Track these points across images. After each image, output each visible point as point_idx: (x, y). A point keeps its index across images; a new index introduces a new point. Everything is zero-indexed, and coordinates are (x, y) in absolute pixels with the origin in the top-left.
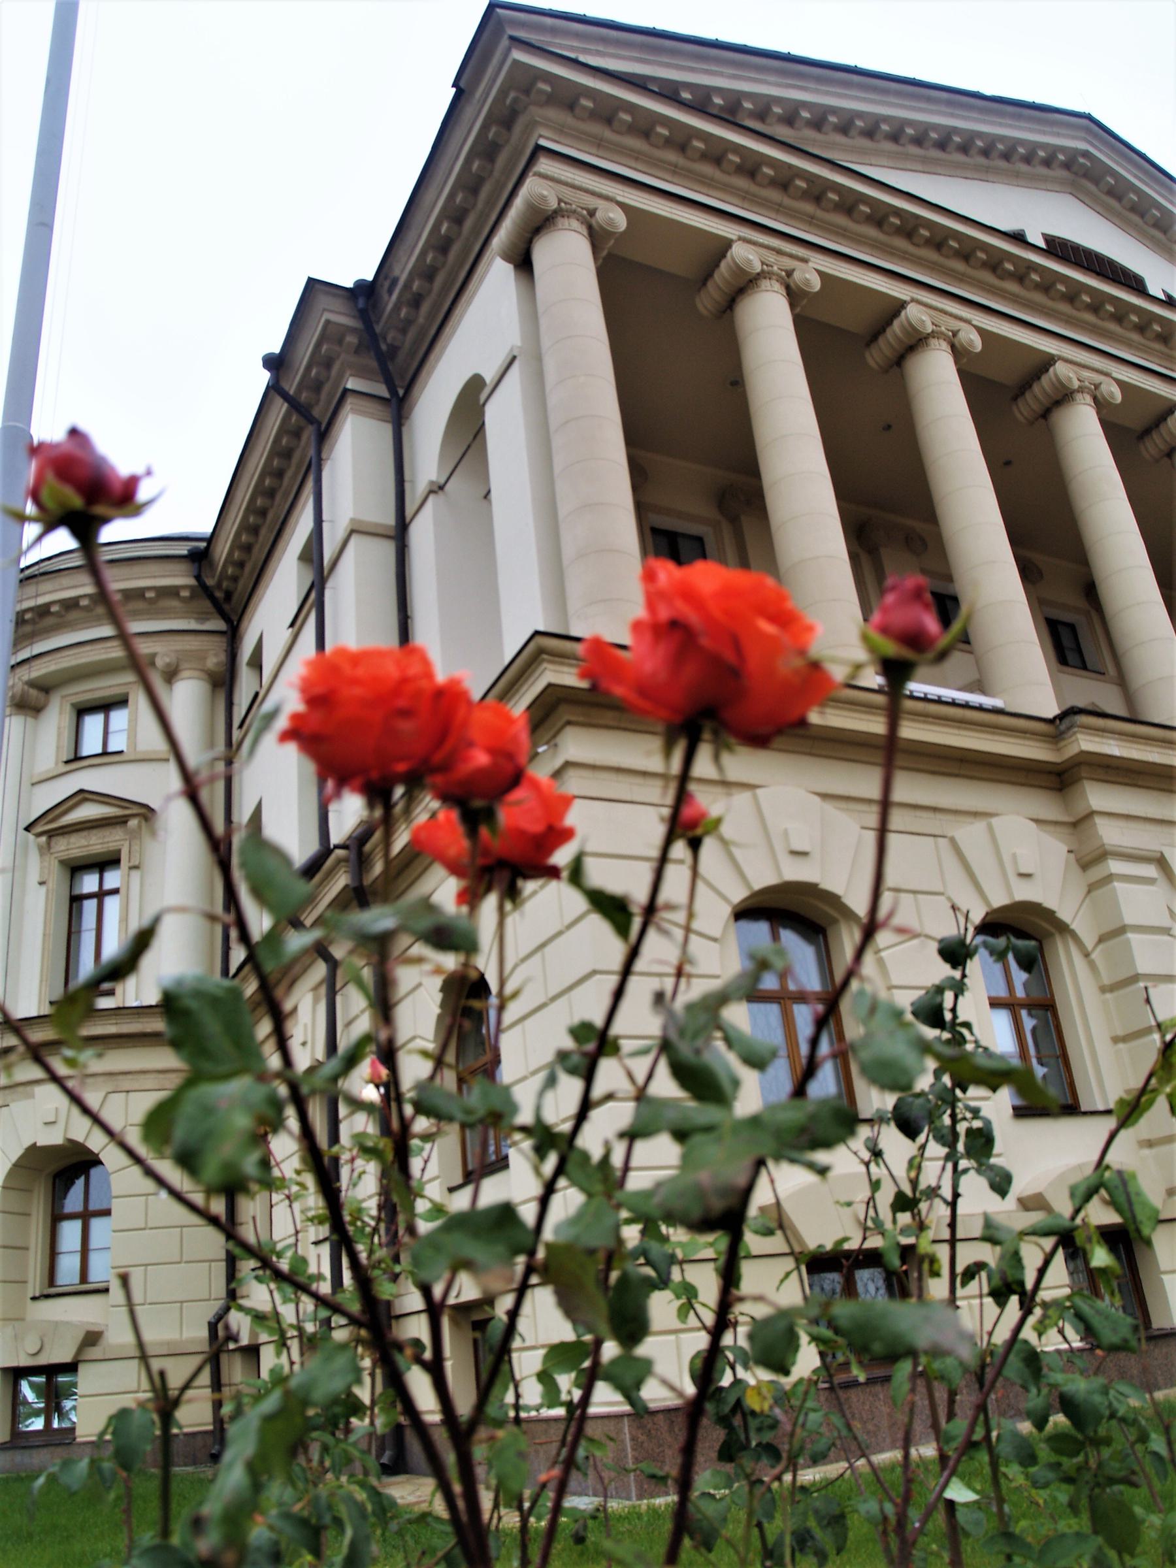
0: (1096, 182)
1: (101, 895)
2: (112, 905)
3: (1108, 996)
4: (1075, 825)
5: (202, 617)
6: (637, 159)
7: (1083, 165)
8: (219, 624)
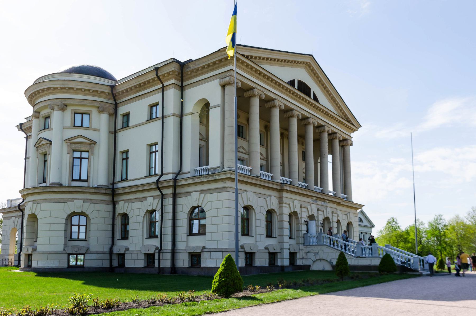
1: (81, 158)
2: (85, 162)
4: (280, 197)
5: (108, 99)
8: (112, 101)
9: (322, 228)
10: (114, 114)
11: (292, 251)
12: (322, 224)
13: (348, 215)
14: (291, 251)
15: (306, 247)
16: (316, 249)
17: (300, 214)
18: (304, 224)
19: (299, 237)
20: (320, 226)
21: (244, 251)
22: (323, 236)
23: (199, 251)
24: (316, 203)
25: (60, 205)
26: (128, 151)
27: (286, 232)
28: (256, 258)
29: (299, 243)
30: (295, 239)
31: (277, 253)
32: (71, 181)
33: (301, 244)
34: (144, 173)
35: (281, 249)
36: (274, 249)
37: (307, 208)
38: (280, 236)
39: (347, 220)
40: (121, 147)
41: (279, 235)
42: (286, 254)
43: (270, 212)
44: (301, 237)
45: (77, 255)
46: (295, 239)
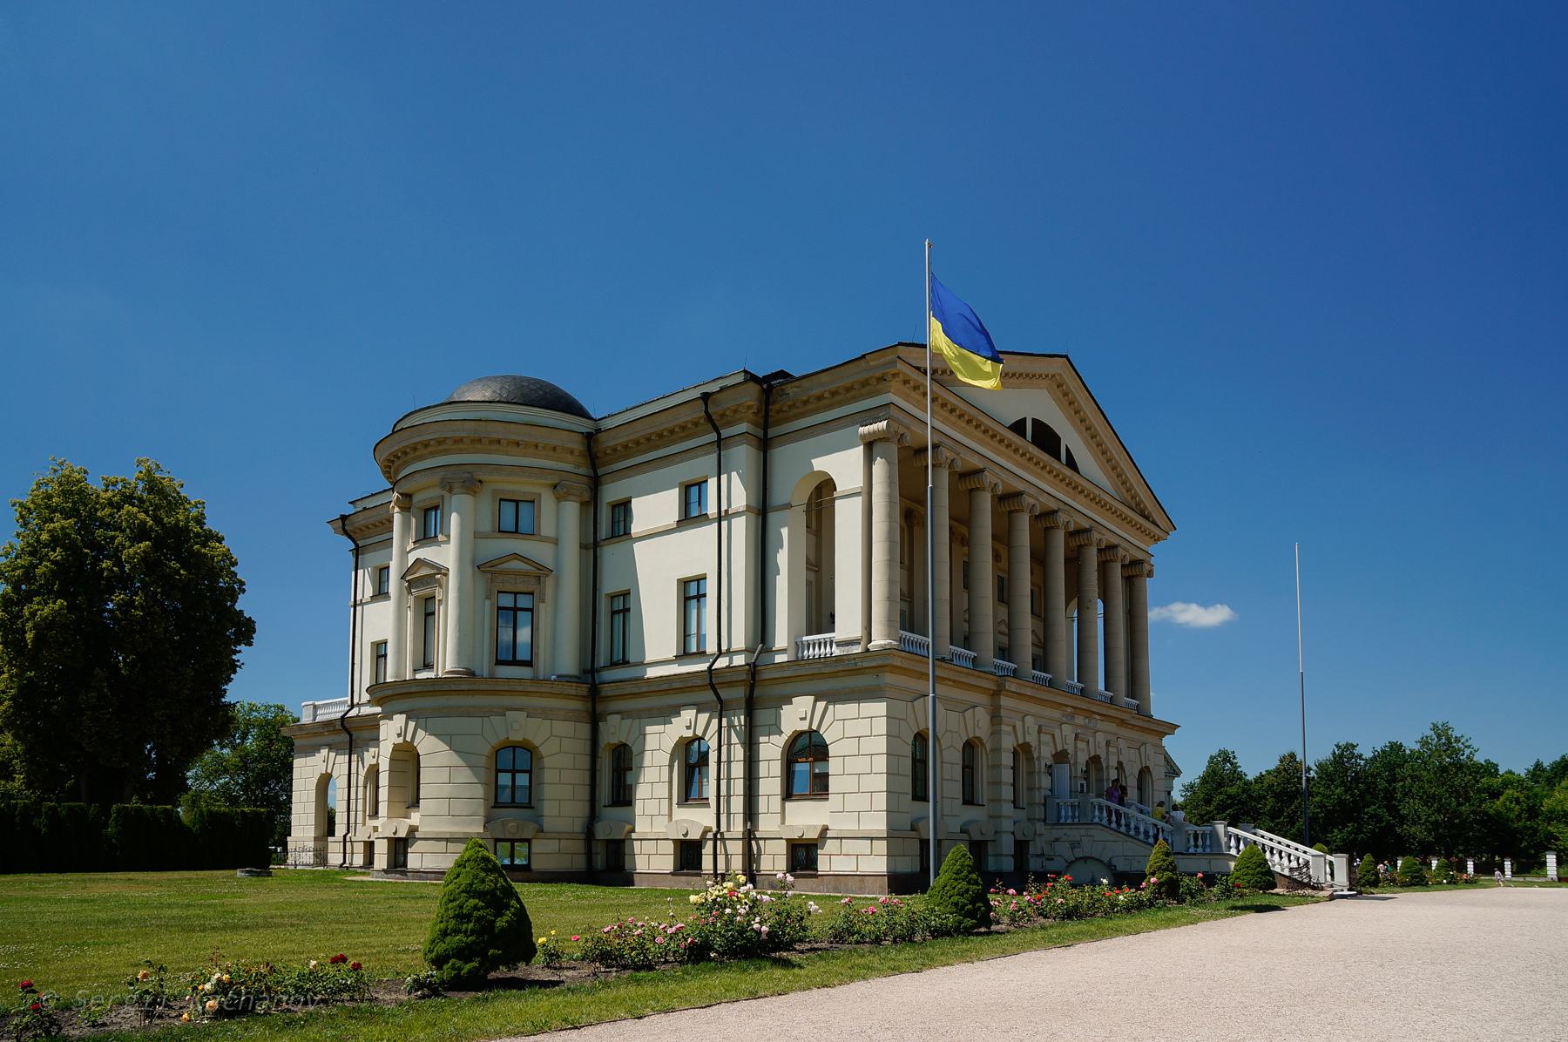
1: (515, 610)
9: (1085, 783)
10: (591, 503)
11: (1020, 837)
12: (1085, 772)
13: (1142, 749)
14: (1018, 838)
15: (1049, 827)
16: (1075, 834)
19: (1035, 804)
22: (1092, 803)
23: (814, 835)
24: (1072, 722)
25: (474, 724)
26: (629, 594)
27: (1007, 792)
29: (1034, 819)
32: (496, 664)
33: (1039, 820)
34: (671, 651)
35: (996, 832)
36: (982, 834)
37: (1053, 735)
38: (993, 801)
39: (1139, 762)
40: (610, 585)
42: (1007, 845)
43: (970, 747)
44: (1039, 804)
45: (513, 841)
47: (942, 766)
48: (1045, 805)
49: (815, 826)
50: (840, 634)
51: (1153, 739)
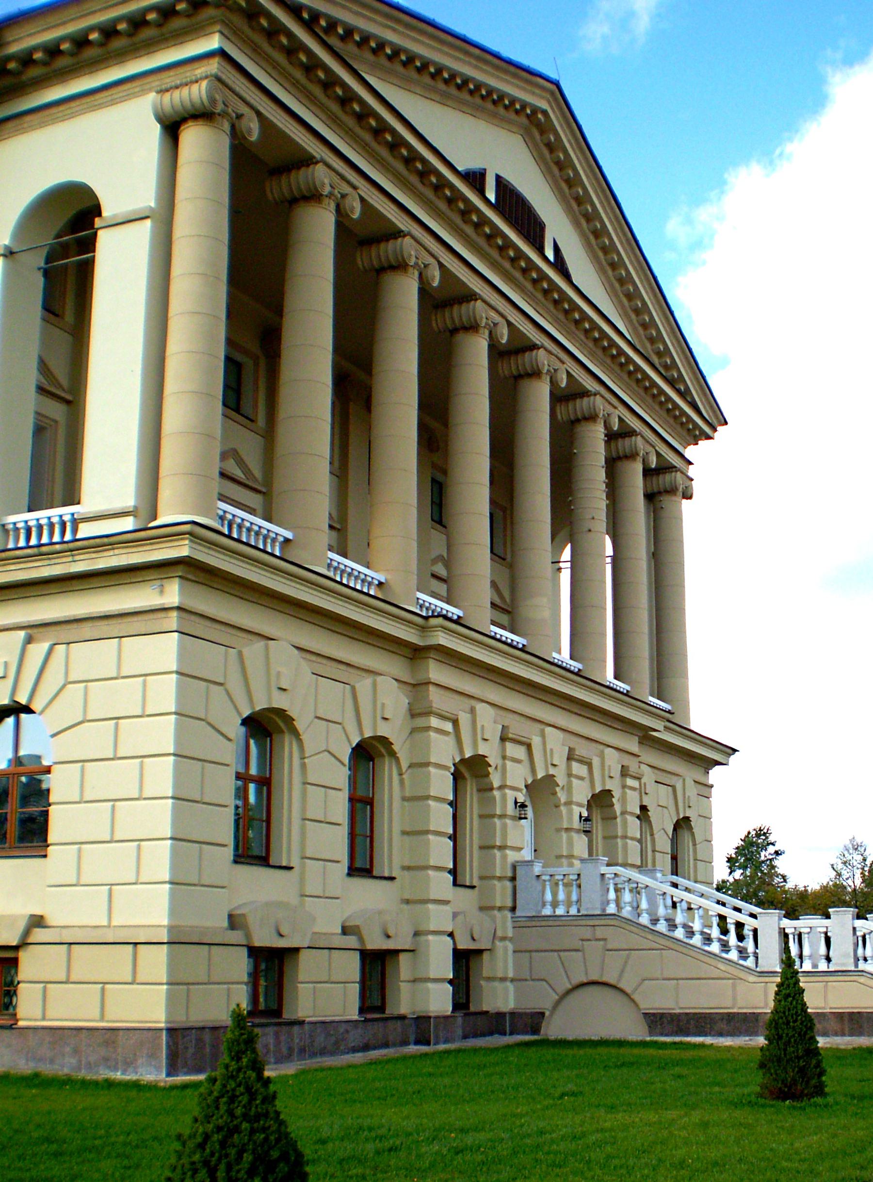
0: (542, 132)
3: (406, 804)
6: (274, 68)
7: (539, 120)
17: (499, 767)
18: (513, 818)
19: (493, 877)
20: (578, 831)
21: (245, 943)
28: (301, 977)
29: (492, 908)
30: (473, 887)
31: (395, 953)
35: (416, 934)
37: (529, 747)
38: (408, 868)
41: (406, 864)
44: (500, 878)
46: (473, 887)
47: (304, 793)
48: (513, 879)
49: (13, 918)
50: (89, 504)
51: (689, 773)
